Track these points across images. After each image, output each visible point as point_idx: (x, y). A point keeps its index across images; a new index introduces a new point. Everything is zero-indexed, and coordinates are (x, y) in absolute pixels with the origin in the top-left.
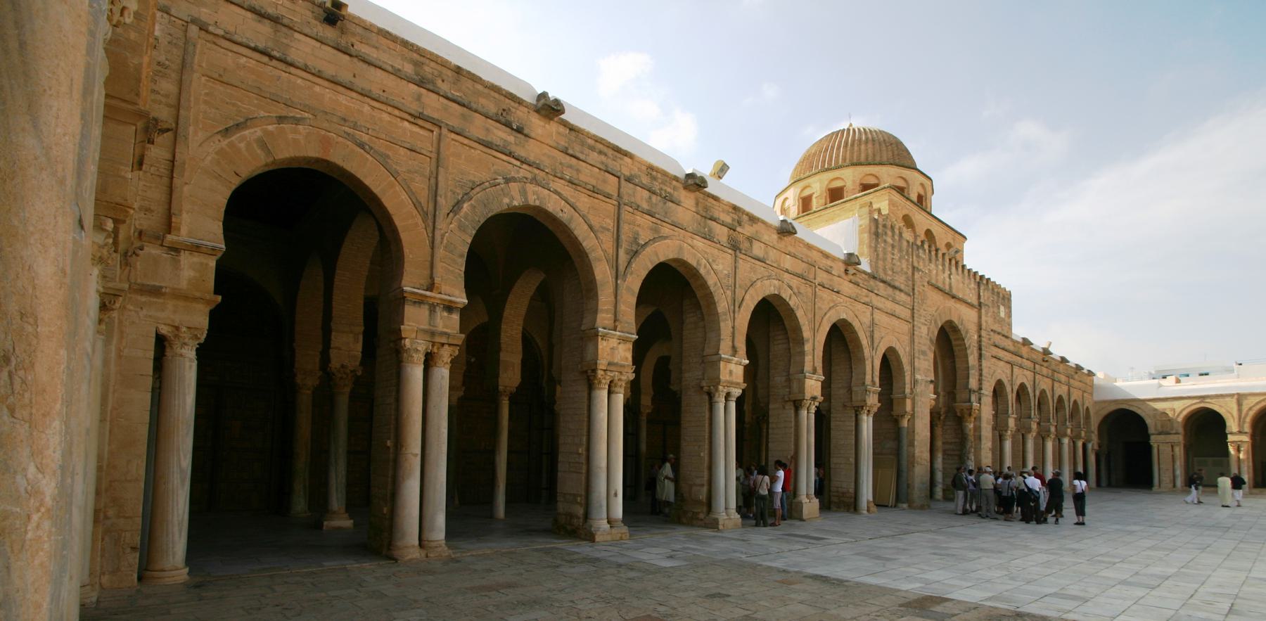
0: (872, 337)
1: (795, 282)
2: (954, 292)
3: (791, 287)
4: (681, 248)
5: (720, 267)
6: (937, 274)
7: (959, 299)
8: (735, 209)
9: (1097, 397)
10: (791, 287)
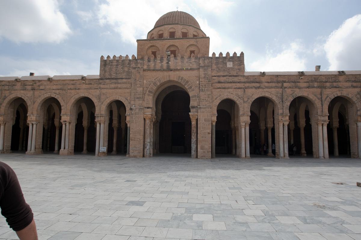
0: (99, 98)
1: (57, 92)
2: (172, 68)
3: (55, 93)
5: (29, 95)
6: (155, 65)
8: (33, 81)
10: (55, 93)
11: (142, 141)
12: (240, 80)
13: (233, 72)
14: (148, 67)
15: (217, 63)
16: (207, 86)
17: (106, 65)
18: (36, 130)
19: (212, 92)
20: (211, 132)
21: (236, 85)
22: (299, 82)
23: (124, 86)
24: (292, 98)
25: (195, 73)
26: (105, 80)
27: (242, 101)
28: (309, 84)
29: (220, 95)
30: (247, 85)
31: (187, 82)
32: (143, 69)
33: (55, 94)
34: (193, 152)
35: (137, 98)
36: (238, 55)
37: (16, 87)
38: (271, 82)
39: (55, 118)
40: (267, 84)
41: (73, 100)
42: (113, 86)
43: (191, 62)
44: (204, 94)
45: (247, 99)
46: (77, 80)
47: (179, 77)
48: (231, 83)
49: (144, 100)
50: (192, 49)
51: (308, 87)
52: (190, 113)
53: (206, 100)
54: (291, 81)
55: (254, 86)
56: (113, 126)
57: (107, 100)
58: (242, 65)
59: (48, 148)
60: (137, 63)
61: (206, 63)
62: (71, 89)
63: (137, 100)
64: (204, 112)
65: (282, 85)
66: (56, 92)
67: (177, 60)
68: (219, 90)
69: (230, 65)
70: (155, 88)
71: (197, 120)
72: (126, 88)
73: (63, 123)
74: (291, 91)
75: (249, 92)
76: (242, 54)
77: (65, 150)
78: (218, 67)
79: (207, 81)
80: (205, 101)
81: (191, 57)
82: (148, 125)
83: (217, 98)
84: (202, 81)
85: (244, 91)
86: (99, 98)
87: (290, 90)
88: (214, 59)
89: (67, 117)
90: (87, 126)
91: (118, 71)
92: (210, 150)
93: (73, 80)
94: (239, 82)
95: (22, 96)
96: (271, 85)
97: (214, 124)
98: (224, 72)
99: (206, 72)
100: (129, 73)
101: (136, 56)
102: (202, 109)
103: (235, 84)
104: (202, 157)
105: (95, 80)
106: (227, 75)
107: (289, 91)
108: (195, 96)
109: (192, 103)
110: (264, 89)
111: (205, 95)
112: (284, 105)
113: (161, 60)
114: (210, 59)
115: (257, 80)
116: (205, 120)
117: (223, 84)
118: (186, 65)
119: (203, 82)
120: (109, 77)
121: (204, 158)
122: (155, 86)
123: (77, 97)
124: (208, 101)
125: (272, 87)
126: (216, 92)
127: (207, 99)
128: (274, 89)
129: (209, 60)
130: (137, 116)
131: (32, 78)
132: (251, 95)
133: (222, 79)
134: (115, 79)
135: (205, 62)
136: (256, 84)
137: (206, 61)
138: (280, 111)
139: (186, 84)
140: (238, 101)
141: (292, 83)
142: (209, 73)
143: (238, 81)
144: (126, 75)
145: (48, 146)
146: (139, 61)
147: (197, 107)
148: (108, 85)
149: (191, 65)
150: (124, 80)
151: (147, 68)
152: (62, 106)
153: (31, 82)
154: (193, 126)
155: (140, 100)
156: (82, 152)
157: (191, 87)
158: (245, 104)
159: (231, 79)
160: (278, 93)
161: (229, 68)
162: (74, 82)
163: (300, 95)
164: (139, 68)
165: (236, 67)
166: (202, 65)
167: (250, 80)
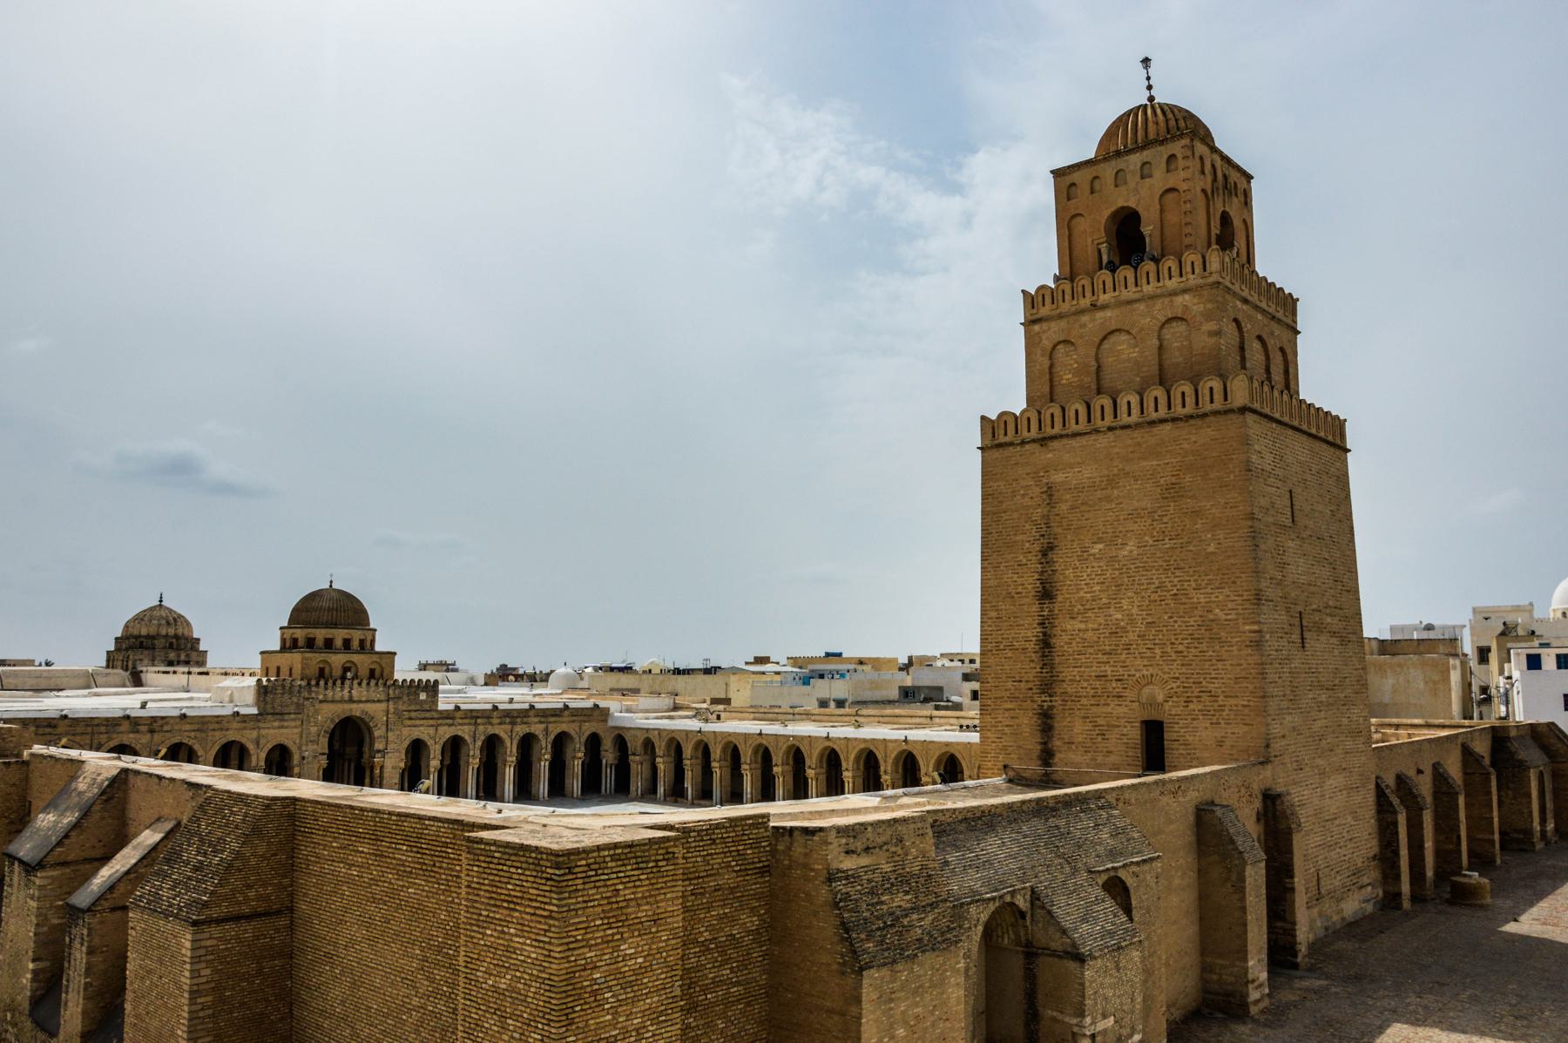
0: (258, 744)
9: (611, 723)
25: (383, 706)
37: (122, 729)
60: (310, 692)
69: (423, 696)
75: (442, 730)
100: (298, 705)
109: (379, 746)
123: (224, 741)
126: (406, 731)
131: (143, 713)
133: (413, 715)
140: (430, 742)
159: (423, 715)
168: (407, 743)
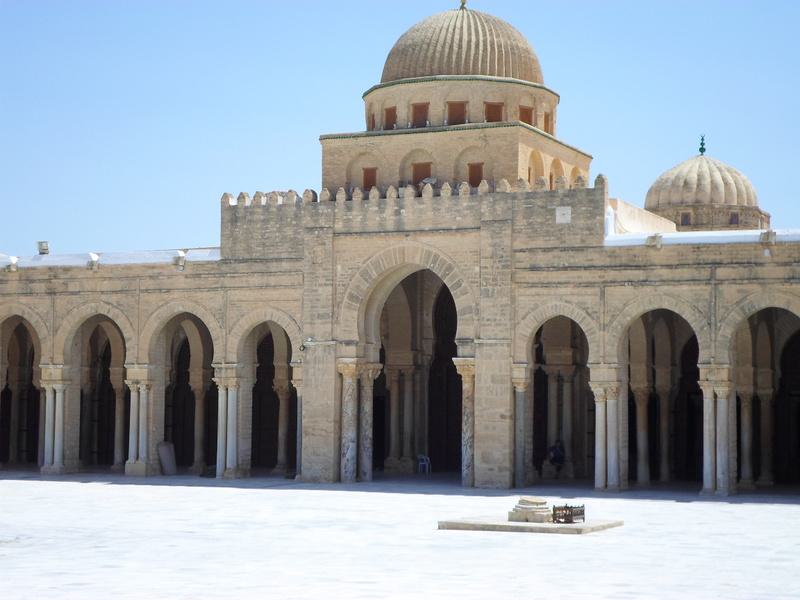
0: (222, 316)
1: (114, 298)
2: (407, 228)
3: (109, 304)
4: (11, 308)
5: (41, 309)
6: (364, 219)
7: (422, 231)
8: (50, 269)
10: (109, 304)
11: (332, 437)
12: (590, 263)
13: (572, 237)
14: (345, 227)
15: (529, 213)
16: (499, 282)
17: (236, 221)
18: (64, 407)
19: (513, 299)
20: (508, 414)
21: (579, 277)
22: (761, 264)
23: (285, 280)
24: (739, 314)
25: (468, 241)
26: (236, 265)
27: (594, 324)
28: (794, 271)
29: (536, 306)
30: (611, 275)
31: (450, 268)
32: (331, 231)
33: (108, 307)
34: (465, 471)
35: (319, 316)
36: (591, 185)
38: (677, 266)
39: (112, 363)
40: (665, 273)
41: (154, 324)
42: (256, 280)
43: (460, 208)
44: (491, 304)
45: (607, 319)
46: (162, 267)
47: (429, 253)
48: (565, 268)
49: (337, 322)
50: (475, 158)
51: (789, 280)
52: (454, 359)
53: (497, 322)
54: (740, 261)
55: (632, 278)
56: (275, 388)
57: (242, 321)
58: (596, 215)
59: (95, 456)
60: (315, 215)
61: (499, 213)
62: (147, 290)
63: (320, 321)
64: (490, 357)
65: (712, 275)
66: (110, 301)
67: (423, 203)
68: (534, 291)
69: (564, 215)
70: (365, 286)
71: (474, 376)
72: (292, 286)
73: (133, 389)
74: (739, 291)
75: (617, 294)
76: (600, 180)
77: (140, 461)
78: (530, 224)
79: (500, 265)
80: (493, 324)
81: (460, 194)
82: (351, 390)
83: (527, 314)
84: (486, 267)
85: (603, 294)
86: (222, 316)
87: (735, 288)
88: (520, 197)
89: (141, 373)
90: (201, 387)
91: (268, 238)
92: (507, 464)
93: (153, 267)
94: (586, 268)
95: (23, 312)
96: (679, 273)
97: (520, 389)
98: (547, 238)
99: (498, 240)
100: (296, 243)
101: (319, 192)
102: (485, 348)
103: (575, 274)
104: (486, 482)
105: (210, 266)
106: (556, 248)
107: (729, 292)
108: (469, 310)
110: (659, 288)
111: (493, 306)
112: (713, 335)
113: (379, 205)
114: (509, 201)
115: (640, 261)
116: (493, 380)
117: (545, 273)
118: (447, 219)
119: (490, 270)
120: (247, 256)
121: (490, 486)
122: (366, 280)
124: (500, 325)
125: (679, 282)
126: (525, 298)
127: (498, 318)
128: (685, 288)
129: (506, 202)
130: (321, 366)
132: (620, 306)
133: (541, 259)
134: (262, 261)
135: (495, 210)
136: (637, 272)
137: (500, 207)
138: (703, 355)
139: (445, 275)
141: (741, 268)
142: (507, 241)
143: (587, 264)
144: (290, 250)
145: (95, 449)
146: (322, 209)
147: (473, 341)
148: (244, 279)
149: (458, 218)
150: (285, 265)
151: (343, 230)
152: (130, 339)
153: (44, 274)
154: (464, 396)
155: (326, 323)
156: (191, 468)
157: (459, 285)
158: (602, 332)
159: (566, 259)
160: (698, 301)
161: (562, 227)
162: (156, 271)
163: (764, 305)
164: (322, 228)
165: (581, 222)
166: (487, 217)
167: (618, 262)
168: (528, 329)
